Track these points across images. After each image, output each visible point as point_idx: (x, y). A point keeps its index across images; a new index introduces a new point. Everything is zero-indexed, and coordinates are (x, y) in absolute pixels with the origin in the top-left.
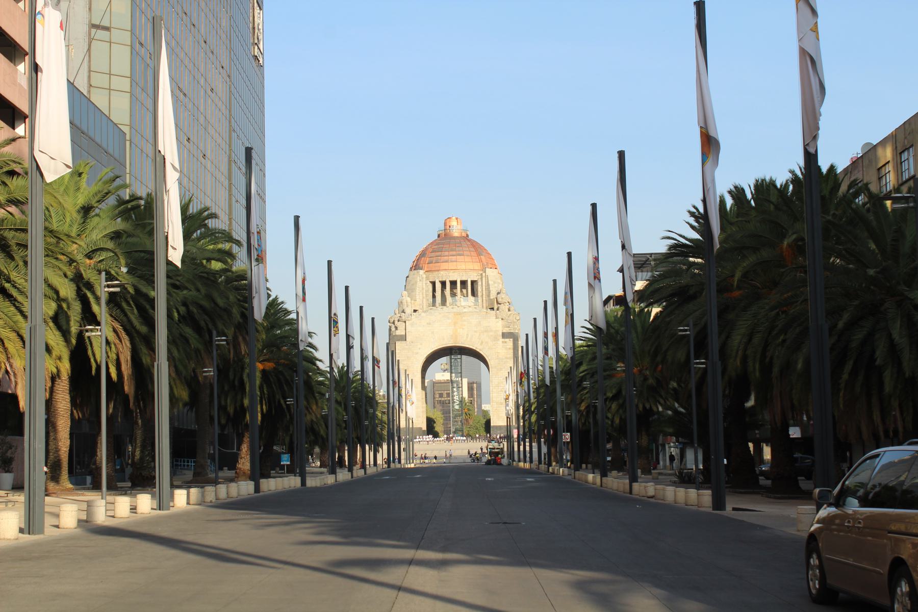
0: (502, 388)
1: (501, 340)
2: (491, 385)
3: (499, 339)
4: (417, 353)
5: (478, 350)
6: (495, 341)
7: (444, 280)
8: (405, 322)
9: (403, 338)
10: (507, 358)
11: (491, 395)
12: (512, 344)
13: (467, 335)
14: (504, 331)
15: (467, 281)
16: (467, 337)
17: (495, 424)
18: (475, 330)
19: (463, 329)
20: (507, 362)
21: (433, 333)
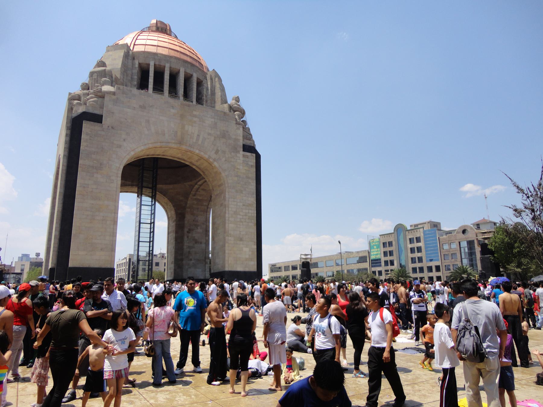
0: (241, 217)
1: (242, 152)
2: (227, 212)
3: (239, 152)
4: (120, 146)
5: (211, 160)
6: (233, 152)
7: (162, 64)
8: (103, 97)
9: (97, 119)
10: (248, 177)
11: (227, 225)
12: (255, 161)
13: (198, 136)
14: (244, 143)
15: (192, 76)
16: (198, 140)
17: (230, 269)
18: (210, 132)
19: (192, 126)
21: (148, 121)
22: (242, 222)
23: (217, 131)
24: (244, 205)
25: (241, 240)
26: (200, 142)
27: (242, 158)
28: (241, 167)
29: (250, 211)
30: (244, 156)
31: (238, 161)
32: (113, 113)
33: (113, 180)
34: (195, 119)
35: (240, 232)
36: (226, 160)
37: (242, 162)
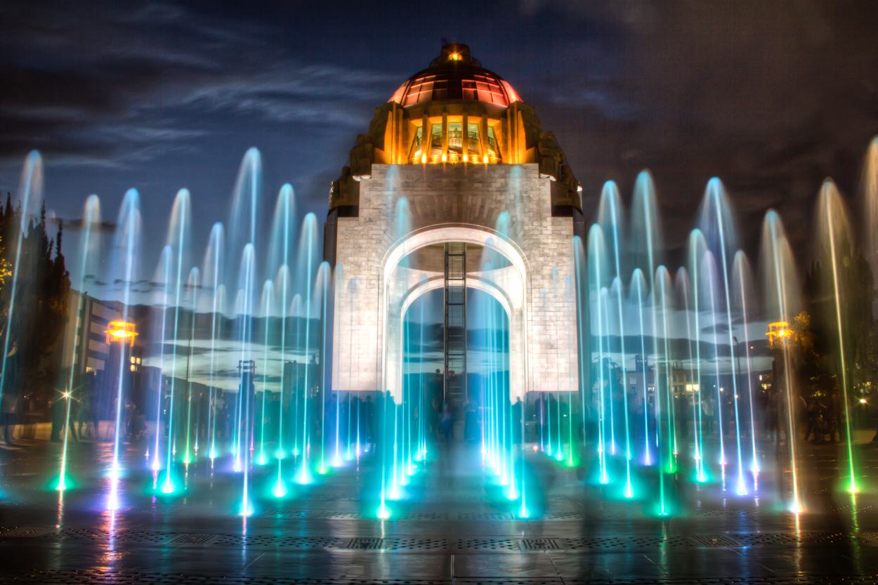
1: (549, 219)
3: (545, 219)
6: (537, 220)
16: (481, 213)
20: (564, 262)
22: (553, 321)
23: (510, 194)
24: (555, 297)
25: (552, 347)
26: (485, 216)
27: (550, 228)
28: (550, 241)
29: (566, 304)
30: (553, 224)
31: (544, 232)
32: (370, 201)
33: (374, 284)
34: (476, 185)
35: (550, 335)
36: (524, 235)
37: (550, 232)
